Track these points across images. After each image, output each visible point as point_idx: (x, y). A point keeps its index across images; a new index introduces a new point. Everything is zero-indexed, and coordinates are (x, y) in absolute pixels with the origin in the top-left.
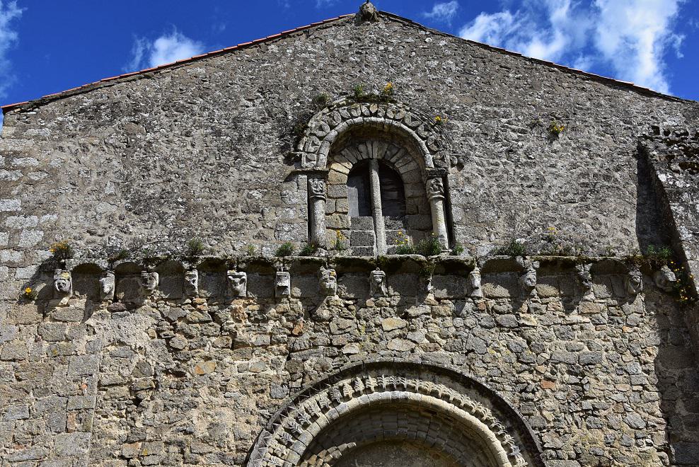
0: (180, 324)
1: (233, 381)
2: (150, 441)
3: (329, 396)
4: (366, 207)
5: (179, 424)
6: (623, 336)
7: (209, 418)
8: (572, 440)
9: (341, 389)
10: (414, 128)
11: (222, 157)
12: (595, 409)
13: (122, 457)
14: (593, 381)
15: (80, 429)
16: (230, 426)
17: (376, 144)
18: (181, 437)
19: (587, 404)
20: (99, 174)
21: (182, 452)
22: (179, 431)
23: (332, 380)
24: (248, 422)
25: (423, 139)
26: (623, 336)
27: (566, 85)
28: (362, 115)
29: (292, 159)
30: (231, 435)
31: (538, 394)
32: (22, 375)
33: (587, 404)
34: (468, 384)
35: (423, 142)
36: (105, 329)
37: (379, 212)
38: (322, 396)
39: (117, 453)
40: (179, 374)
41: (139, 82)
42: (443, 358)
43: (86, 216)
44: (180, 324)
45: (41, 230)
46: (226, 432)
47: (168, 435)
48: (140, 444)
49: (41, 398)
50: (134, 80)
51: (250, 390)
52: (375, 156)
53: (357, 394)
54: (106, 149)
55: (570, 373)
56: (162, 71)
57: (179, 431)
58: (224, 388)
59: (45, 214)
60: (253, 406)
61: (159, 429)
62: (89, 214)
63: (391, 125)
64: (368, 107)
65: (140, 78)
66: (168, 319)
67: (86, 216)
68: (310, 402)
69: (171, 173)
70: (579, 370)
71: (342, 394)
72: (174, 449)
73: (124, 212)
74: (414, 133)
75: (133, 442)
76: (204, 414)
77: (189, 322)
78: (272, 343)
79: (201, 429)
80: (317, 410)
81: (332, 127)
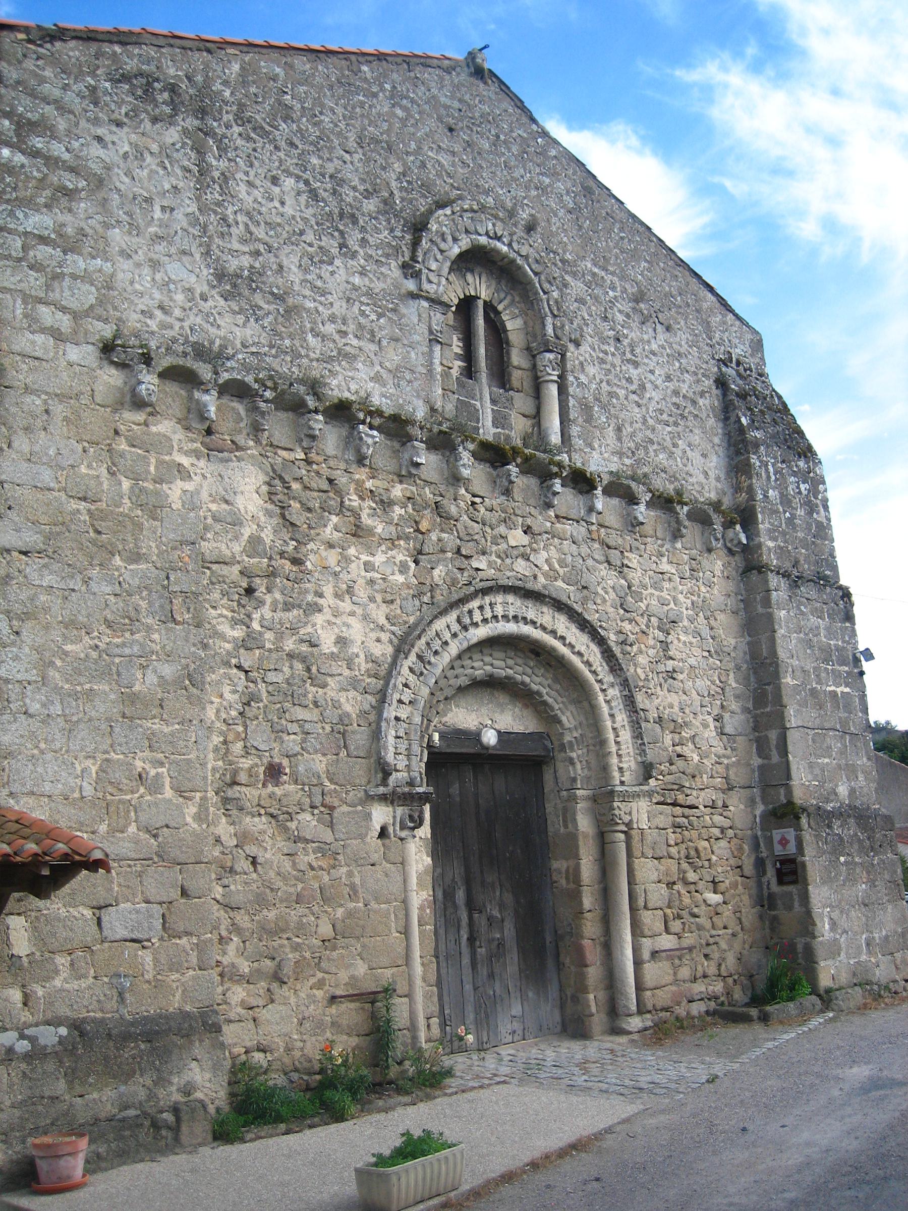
0: (295, 486)
1: (361, 582)
2: (270, 650)
3: (459, 620)
4: (470, 371)
5: (302, 631)
6: (699, 596)
7: (336, 630)
8: (656, 702)
9: (470, 612)
10: (536, 274)
11: (323, 238)
12: (674, 671)
13: (239, 667)
14: (676, 642)
15: (190, 621)
16: (359, 643)
17: (484, 279)
18: (304, 648)
19: (670, 664)
20: (163, 208)
21: (308, 670)
22: (302, 641)
23: (463, 601)
24: (378, 640)
25: (545, 293)
26: (699, 596)
27: (662, 265)
28: (487, 234)
29: (409, 269)
30: (362, 656)
31: (635, 648)
32: (102, 525)
33: (670, 664)
34: (584, 625)
35: (544, 297)
36: (203, 475)
37: (484, 376)
38: (452, 617)
39: (234, 661)
40: (296, 561)
41: (197, 55)
42: (562, 589)
43: (153, 279)
44: (295, 486)
45: (92, 285)
46: (355, 651)
47: (290, 644)
48: (257, 652)
49: (132, 567)
50: (190, 49)
51: (379, 598)
52: (483, 296)
53: (485, 621)
54: (168, 166)
55: (659, 628)
56: (231, 51)
57: (302, 641)
58: (350, 591)
59: (94, 258)
60: (382, 621)
61: (280, 636)
62: (158, 277)
63: (513, 261)
64: (494, 225)
65: (199, 50)
66: (281, 478)
67: (153, 279)
68: (439, 625)
69: (259, 240)
70: (668, 624)
71: (471, 619)
72: (299, 666)
73: (206, 288)
74: (536, 280)
75: (251, 649)
76: (329, 622)
77: (306, 488)
78: (399, 538)
79: (328, 644)
80: (447, 636)
81: (455, 240)
